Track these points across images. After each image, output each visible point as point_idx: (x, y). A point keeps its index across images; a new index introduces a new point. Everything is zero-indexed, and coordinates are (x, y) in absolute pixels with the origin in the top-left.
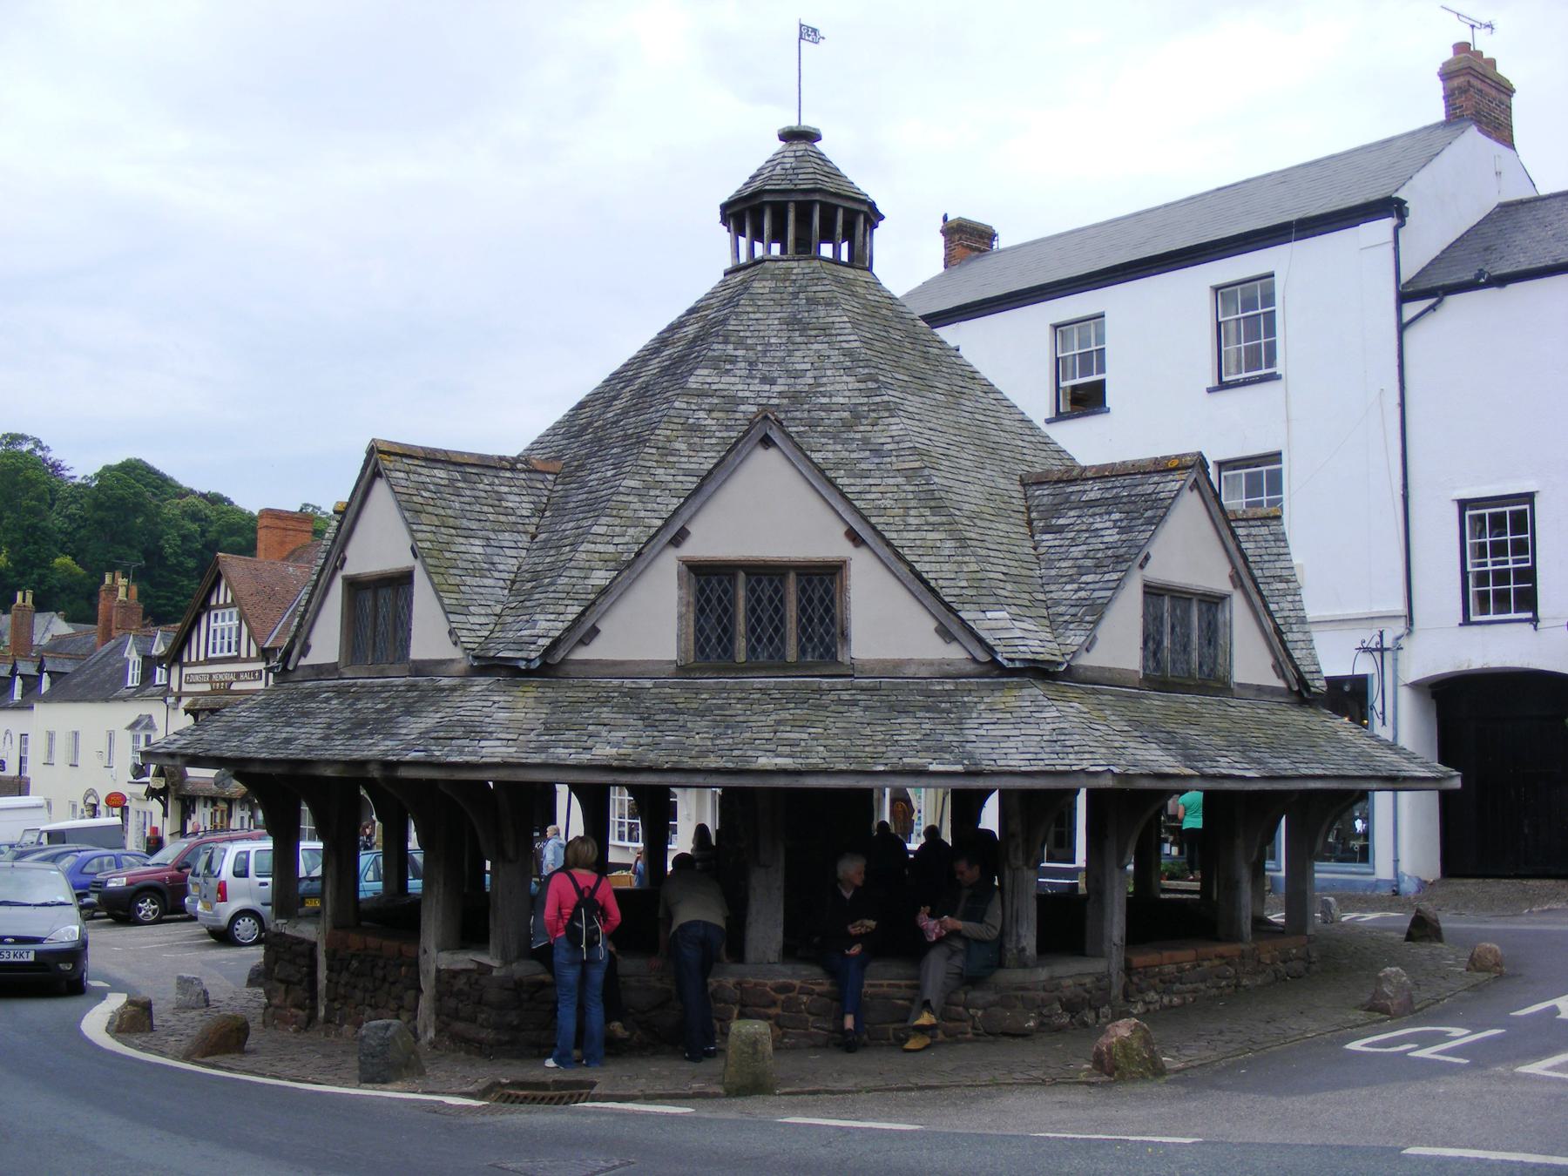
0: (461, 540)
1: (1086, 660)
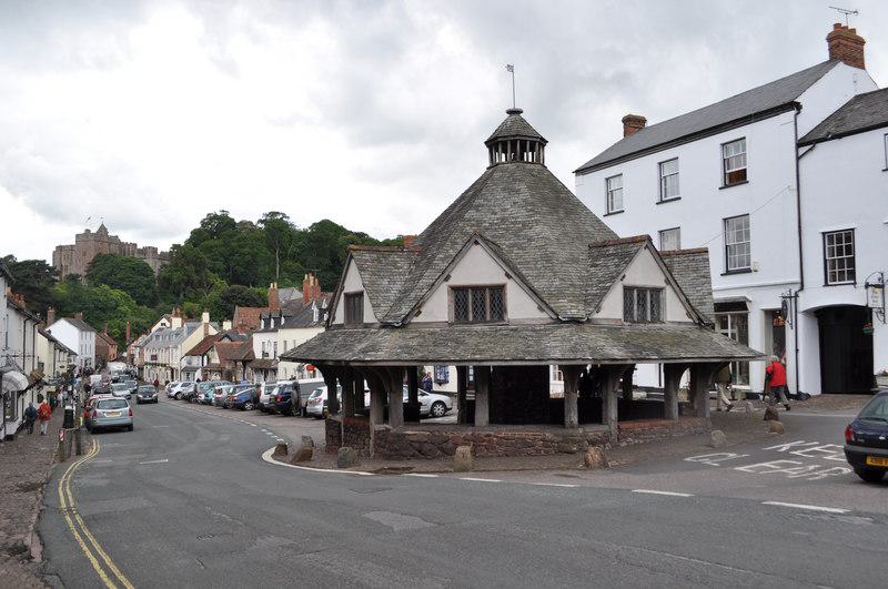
1: (596, 316)
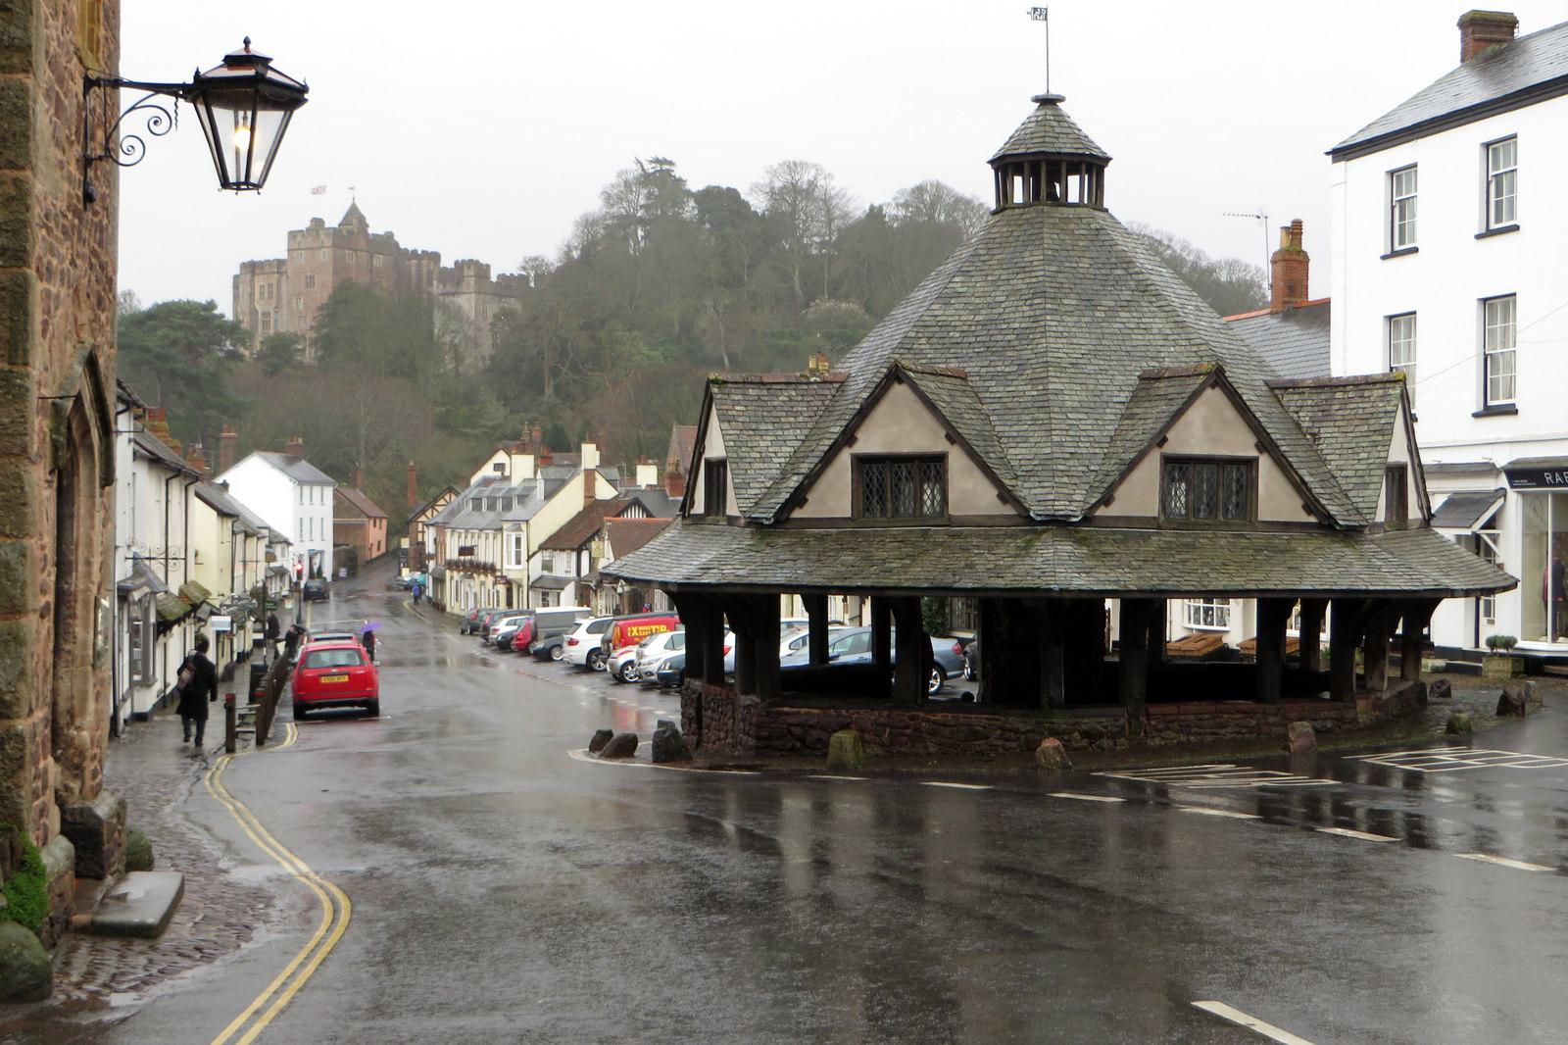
0: (758, 438)
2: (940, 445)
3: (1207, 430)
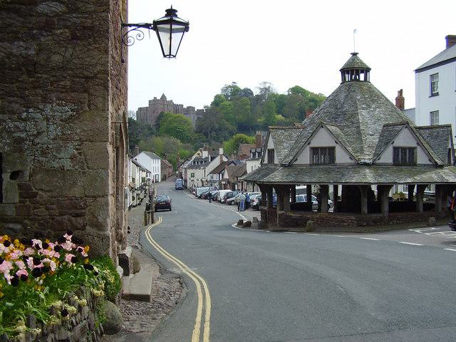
2: (333, 144)
3: (404, 140)
